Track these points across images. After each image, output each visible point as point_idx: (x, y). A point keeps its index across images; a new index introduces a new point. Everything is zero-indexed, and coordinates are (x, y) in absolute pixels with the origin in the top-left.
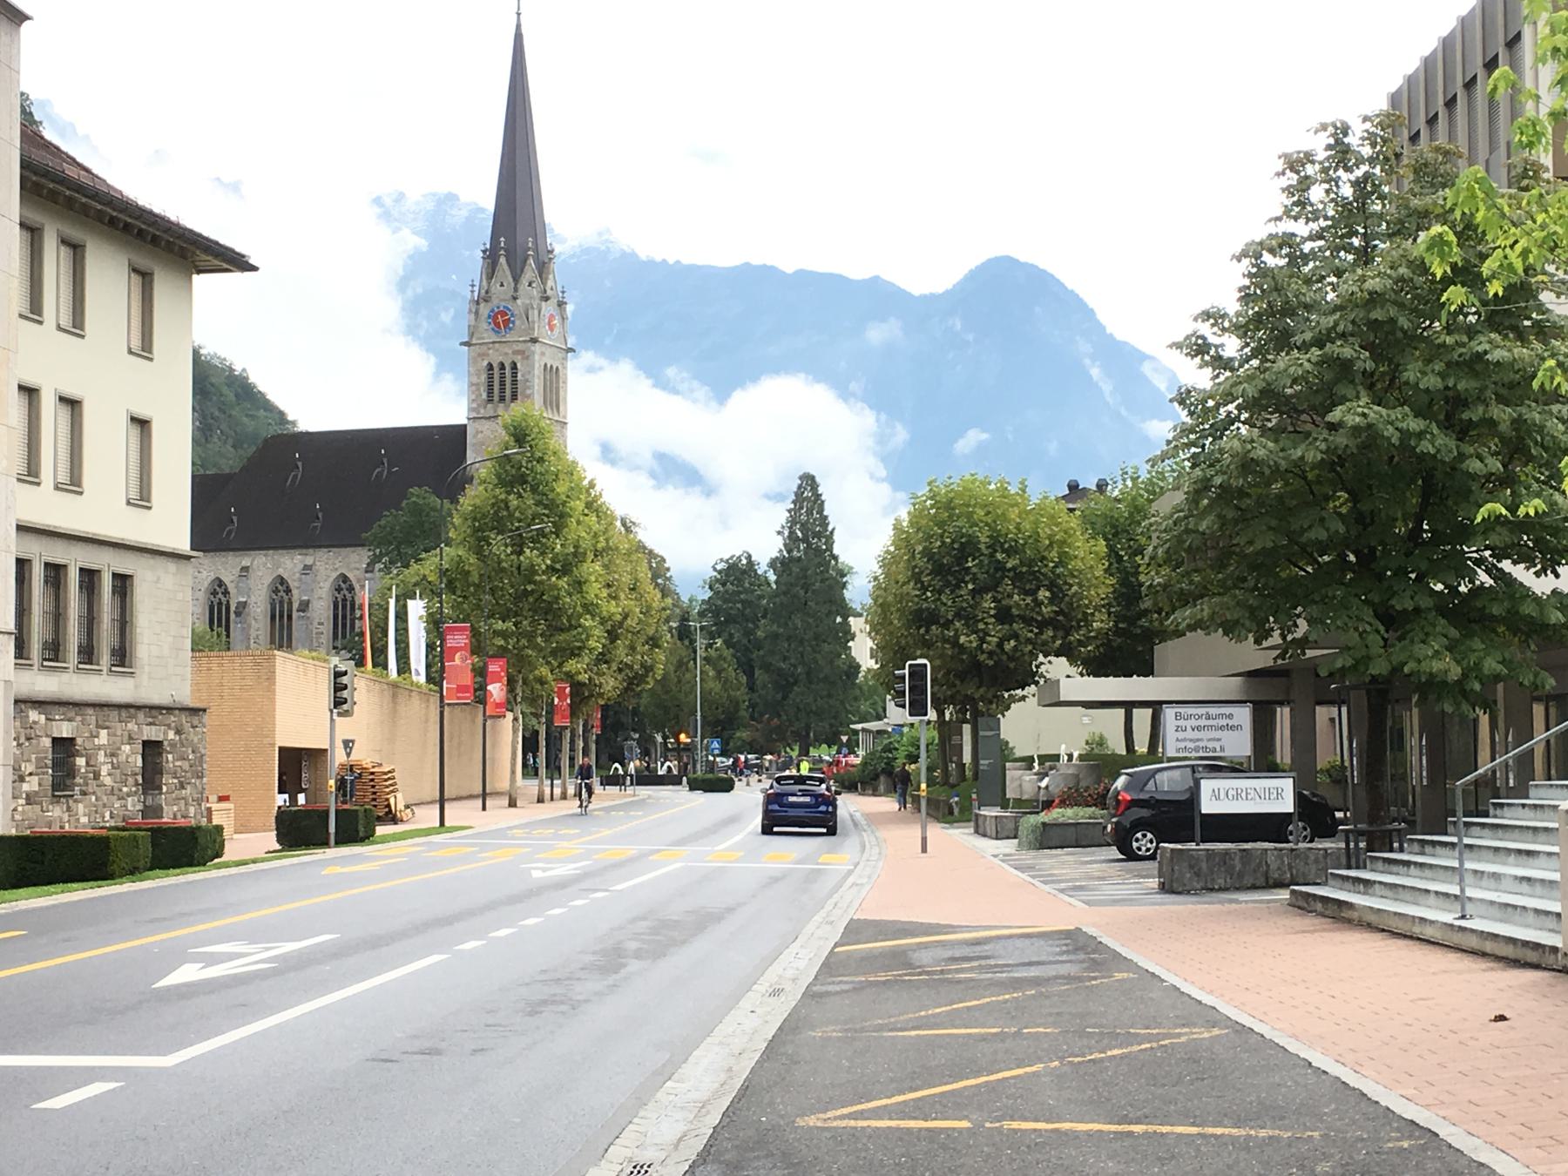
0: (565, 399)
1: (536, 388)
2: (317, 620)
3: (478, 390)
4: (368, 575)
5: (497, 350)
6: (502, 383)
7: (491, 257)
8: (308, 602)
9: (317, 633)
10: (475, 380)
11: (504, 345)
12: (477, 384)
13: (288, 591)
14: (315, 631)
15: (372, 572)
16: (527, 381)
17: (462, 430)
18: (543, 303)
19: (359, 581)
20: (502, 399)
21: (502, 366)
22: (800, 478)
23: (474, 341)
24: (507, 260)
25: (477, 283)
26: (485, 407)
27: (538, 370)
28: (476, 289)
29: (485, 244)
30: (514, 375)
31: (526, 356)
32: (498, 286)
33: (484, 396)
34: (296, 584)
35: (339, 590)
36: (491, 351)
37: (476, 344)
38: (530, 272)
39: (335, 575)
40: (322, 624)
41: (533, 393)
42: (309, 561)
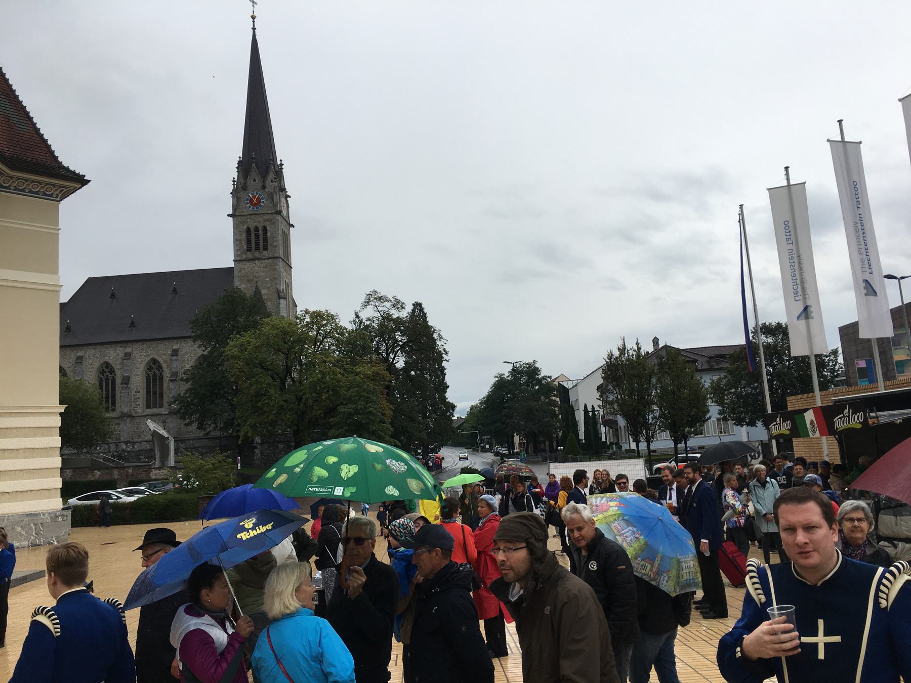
0: (290, 253)
1: (280, 242)
2: (135, 390)
3: (242, 243)
4: (174, 358)
5: (253, 219)
6: (257, 240)
7: (244, 166)
8: (128, 378)
9: (134, 399)
10: (238, 237)
11: (257, 216)
12: (240, 240)
13: (112, 371)
14: (133, 397)
15: (177, 355)
16: (274, 237)
17: (229, 271)
18: (281, 193)
19: (166, 362)
20: (257, 249)
21: (256, 229)
22: (413, 305)
23: (237, 214)
24: (258, 168)
25: (236, 180)
26: (246, 254)
27: (280, 232)
28: (235, 183)
29: (240, 158)
30: (265, 235)
31: (273, 223)
32: (252, 181)
33: (245, 247)
34: (118, 367)
35: (150, 369)
36: (249, 220)
37: (238, 216)
38: (271, 176)
39: (147, 359)
40: (139, 392)
41: (279, 245)
42: (128, 350)
